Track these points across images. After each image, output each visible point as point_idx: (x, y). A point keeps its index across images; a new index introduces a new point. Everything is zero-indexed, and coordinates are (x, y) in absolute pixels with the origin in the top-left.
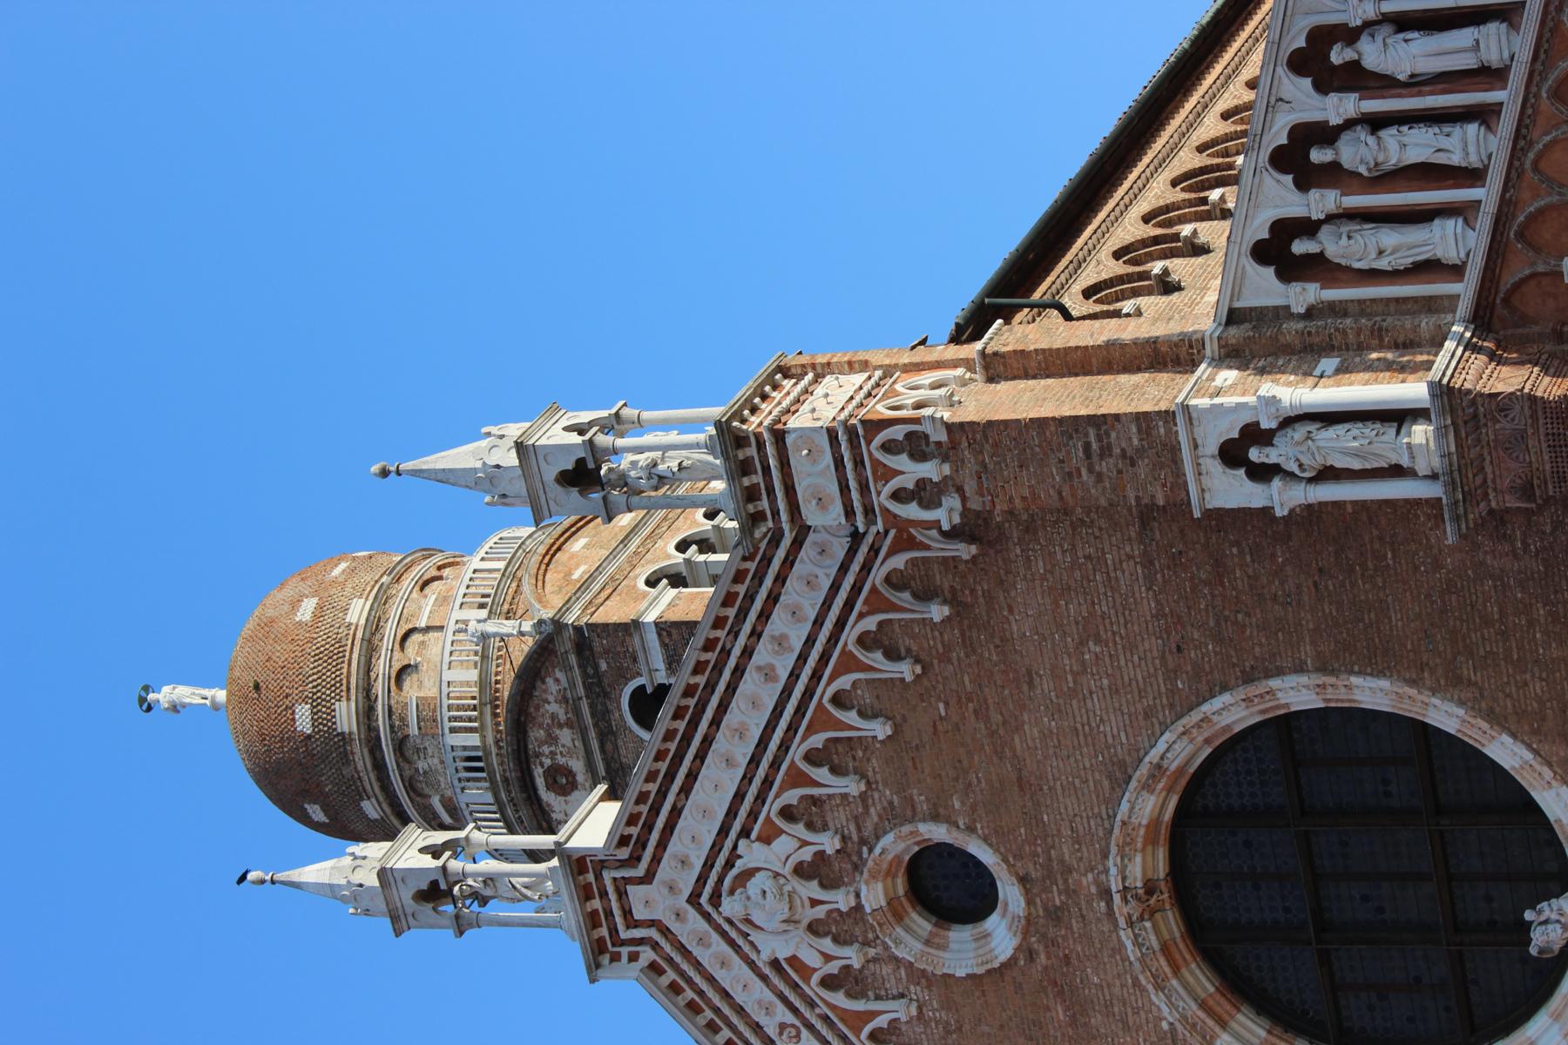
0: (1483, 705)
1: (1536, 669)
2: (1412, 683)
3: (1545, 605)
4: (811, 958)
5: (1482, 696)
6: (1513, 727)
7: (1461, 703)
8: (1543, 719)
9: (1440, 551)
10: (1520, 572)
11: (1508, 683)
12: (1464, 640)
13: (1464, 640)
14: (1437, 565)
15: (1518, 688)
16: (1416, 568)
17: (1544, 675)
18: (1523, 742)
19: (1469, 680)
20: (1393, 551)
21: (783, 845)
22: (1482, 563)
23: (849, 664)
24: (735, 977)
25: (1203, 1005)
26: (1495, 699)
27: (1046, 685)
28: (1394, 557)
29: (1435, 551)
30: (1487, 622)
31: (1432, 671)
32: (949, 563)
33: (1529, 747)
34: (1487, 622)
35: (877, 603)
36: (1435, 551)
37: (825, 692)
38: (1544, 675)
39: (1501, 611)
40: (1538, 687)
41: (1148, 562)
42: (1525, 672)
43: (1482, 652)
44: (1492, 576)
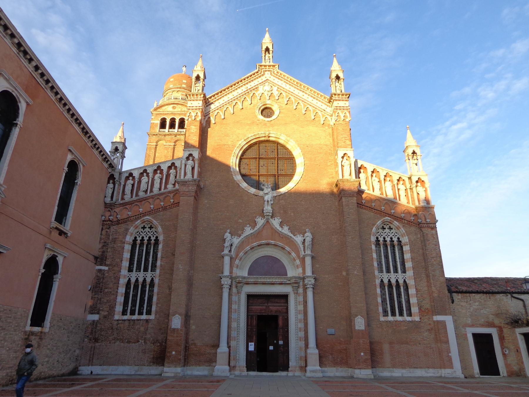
4: (258, 92)
21: (277, 92)
23: (305, 106)
24: (256, 82)
25: (250, 141)
27: (302, 129)
32: (320, 120)
35: (314, 111)
37: (300, 102)
41: (320, 144)
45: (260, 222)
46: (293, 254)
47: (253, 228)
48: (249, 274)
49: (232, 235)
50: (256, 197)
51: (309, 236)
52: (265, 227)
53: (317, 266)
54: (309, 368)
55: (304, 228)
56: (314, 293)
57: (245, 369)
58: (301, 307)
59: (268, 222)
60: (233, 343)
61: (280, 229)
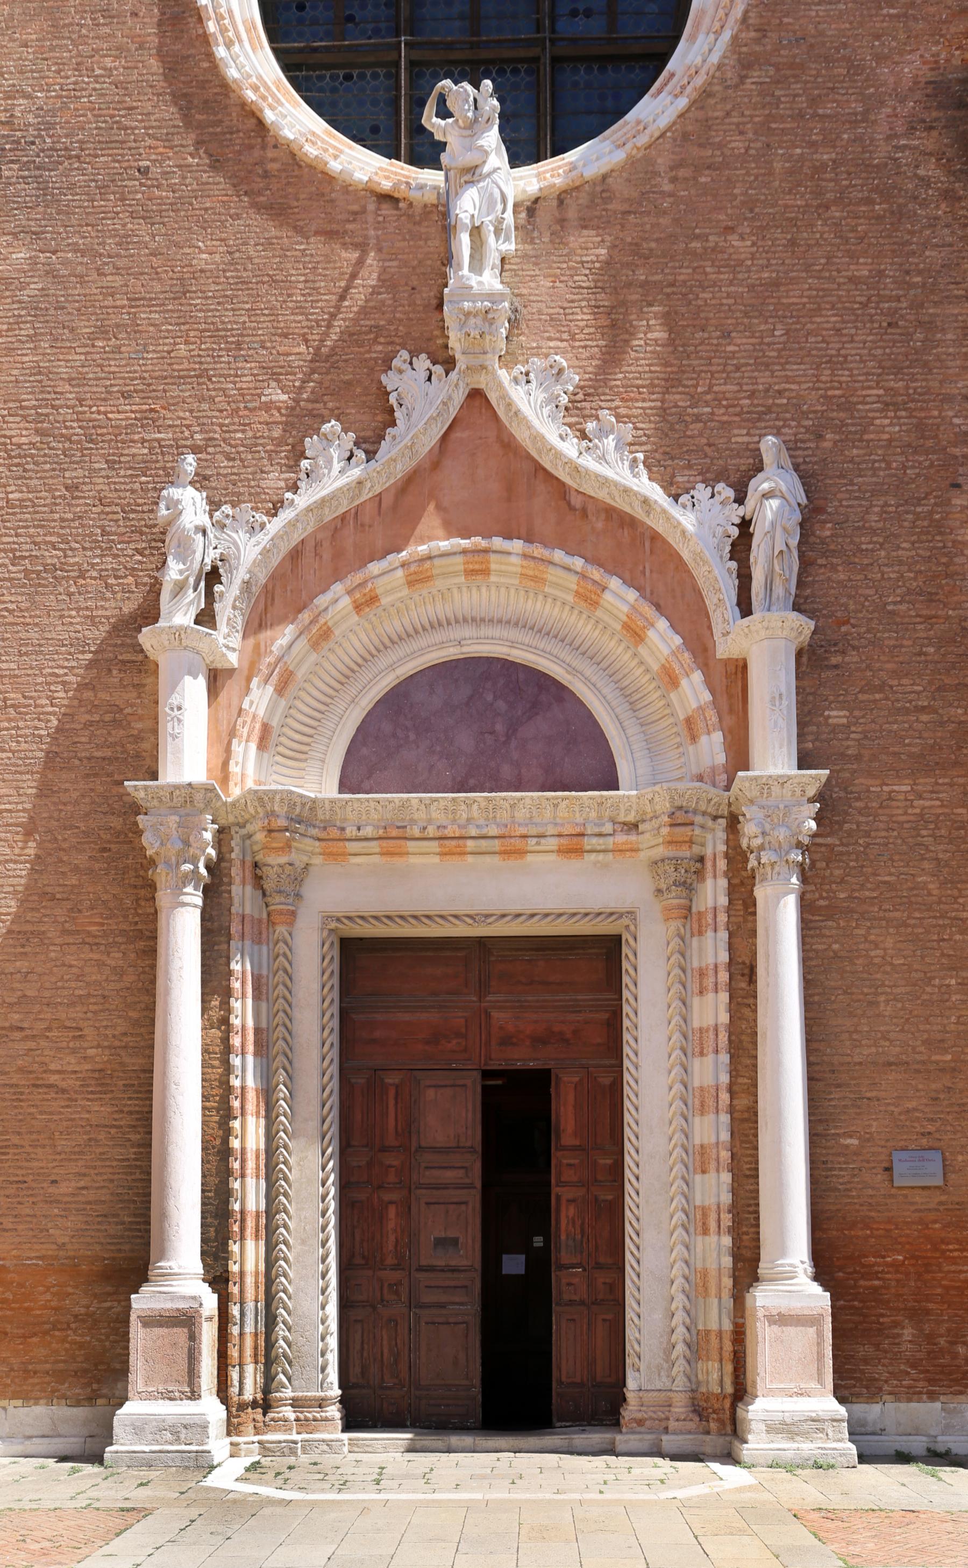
0: (717, 88)
1: (759, 145)
2: (745, 19)
3: (834, 161)
5: (727, 87)
6: (690, 115)
7: (720, 67)
8: (701, 145)
9: (897, 63)
10: (872, 140)
11: (743, 115)
12: (794, 76)
13: (794, 76)
14: (880, 58)
15: (738, 125)
16: (878, 37)
17: (752, 152)
18: (674, 123)
19: (746, 77)
20: (897, 16)
22: (882, 103)
26: (724, 99)
28: (890, 16)
29: (897, 58)
30: (814, 102)
31: (757, 41)
33: (669, 129)
34: (814, 102)
36: (897, 58)
38: (752, 152)
39: (828, 116)
40: (738, 144)
42: (755, 133)
43: (778, 93)
44: (866, 112)
45: (422, 399)
46: (663, 639)
47: (369, 445)
48: (345, 785)
49: (214, 505)
50: (387, 209)
51: (775, 501)
52: (457, 434)
53: (837, 716)
54: (759, 1410)
55: (740, 437)
56: (806, 908)
57: (334, 1412)
58: (713, 1010)
59: (476, 395)
60: (248, 1256)
61: (570, 448)
